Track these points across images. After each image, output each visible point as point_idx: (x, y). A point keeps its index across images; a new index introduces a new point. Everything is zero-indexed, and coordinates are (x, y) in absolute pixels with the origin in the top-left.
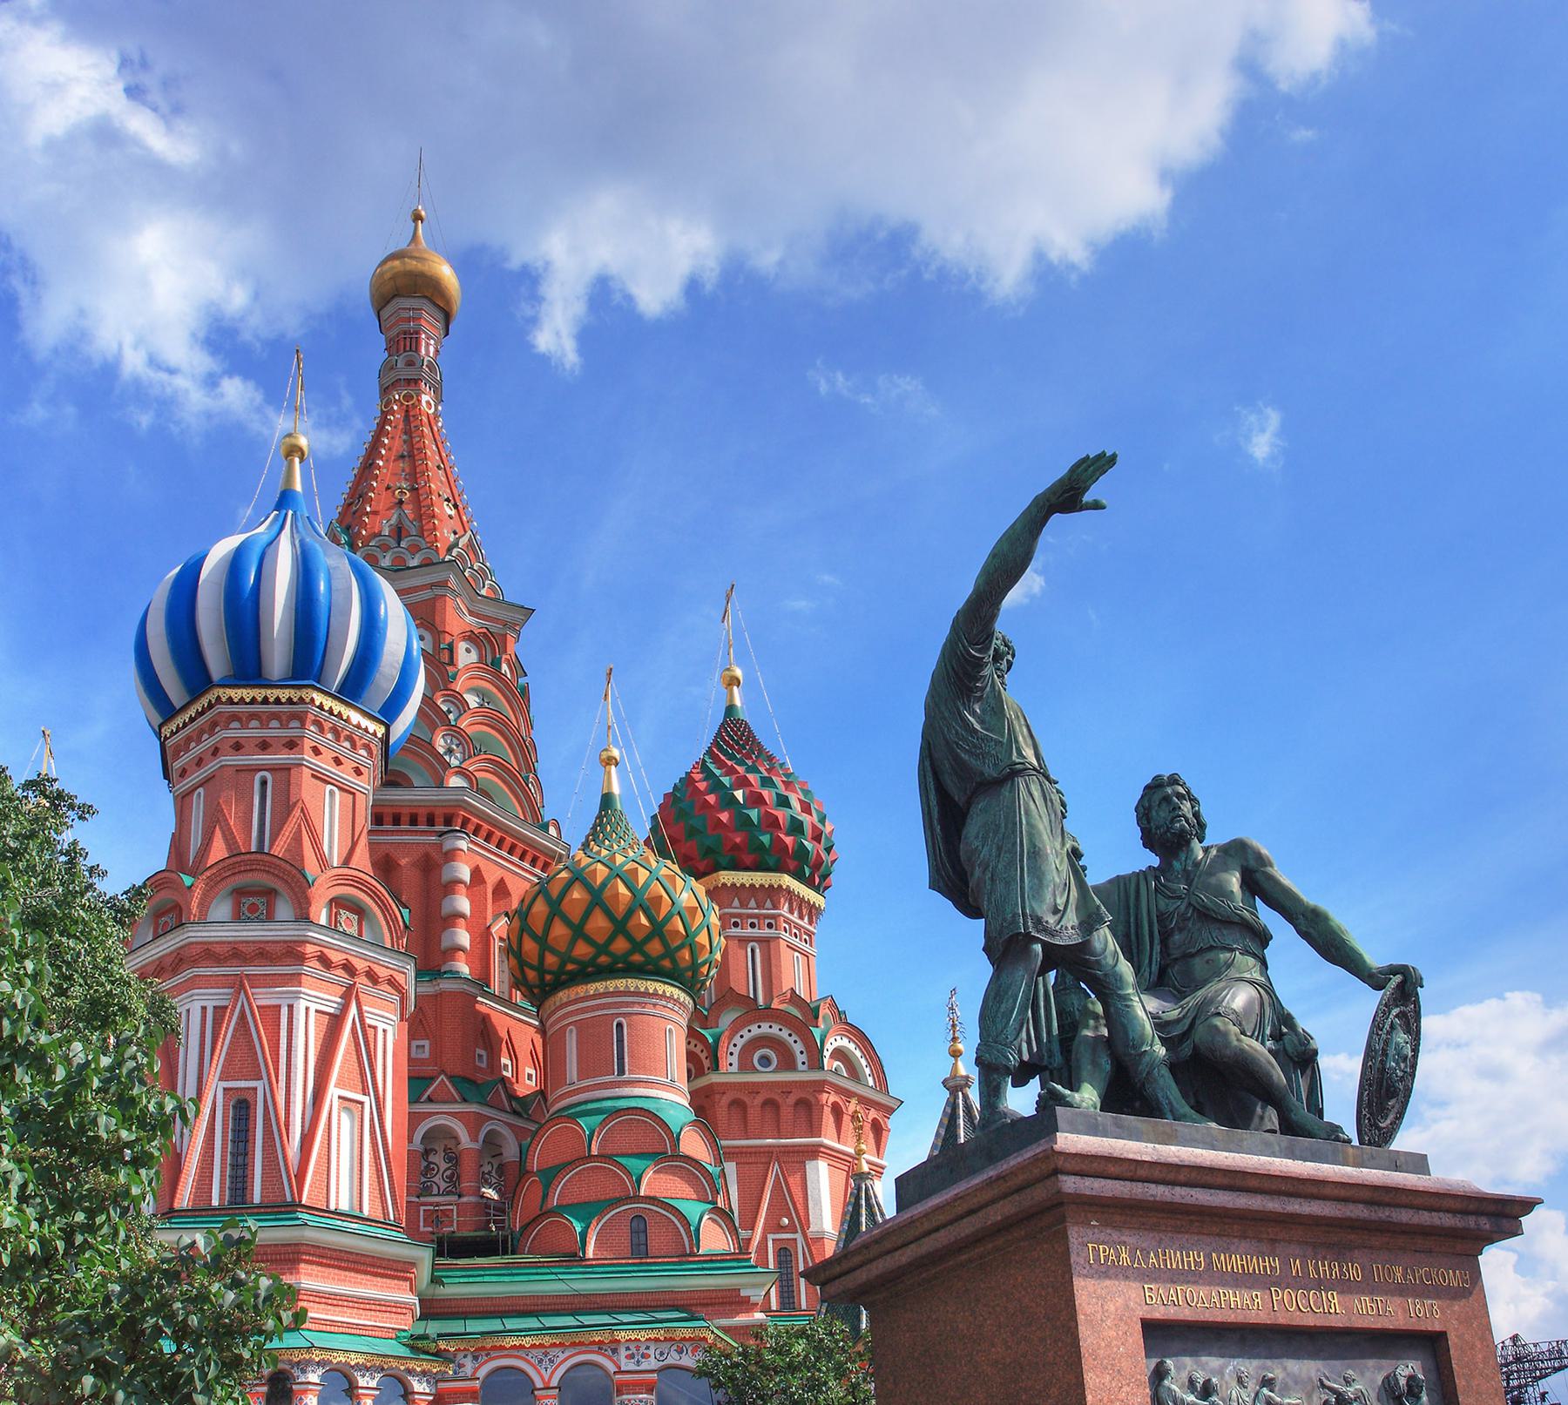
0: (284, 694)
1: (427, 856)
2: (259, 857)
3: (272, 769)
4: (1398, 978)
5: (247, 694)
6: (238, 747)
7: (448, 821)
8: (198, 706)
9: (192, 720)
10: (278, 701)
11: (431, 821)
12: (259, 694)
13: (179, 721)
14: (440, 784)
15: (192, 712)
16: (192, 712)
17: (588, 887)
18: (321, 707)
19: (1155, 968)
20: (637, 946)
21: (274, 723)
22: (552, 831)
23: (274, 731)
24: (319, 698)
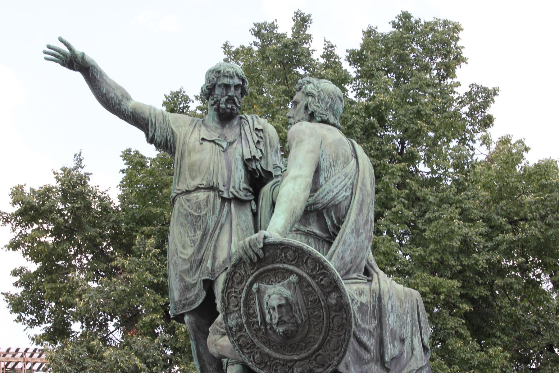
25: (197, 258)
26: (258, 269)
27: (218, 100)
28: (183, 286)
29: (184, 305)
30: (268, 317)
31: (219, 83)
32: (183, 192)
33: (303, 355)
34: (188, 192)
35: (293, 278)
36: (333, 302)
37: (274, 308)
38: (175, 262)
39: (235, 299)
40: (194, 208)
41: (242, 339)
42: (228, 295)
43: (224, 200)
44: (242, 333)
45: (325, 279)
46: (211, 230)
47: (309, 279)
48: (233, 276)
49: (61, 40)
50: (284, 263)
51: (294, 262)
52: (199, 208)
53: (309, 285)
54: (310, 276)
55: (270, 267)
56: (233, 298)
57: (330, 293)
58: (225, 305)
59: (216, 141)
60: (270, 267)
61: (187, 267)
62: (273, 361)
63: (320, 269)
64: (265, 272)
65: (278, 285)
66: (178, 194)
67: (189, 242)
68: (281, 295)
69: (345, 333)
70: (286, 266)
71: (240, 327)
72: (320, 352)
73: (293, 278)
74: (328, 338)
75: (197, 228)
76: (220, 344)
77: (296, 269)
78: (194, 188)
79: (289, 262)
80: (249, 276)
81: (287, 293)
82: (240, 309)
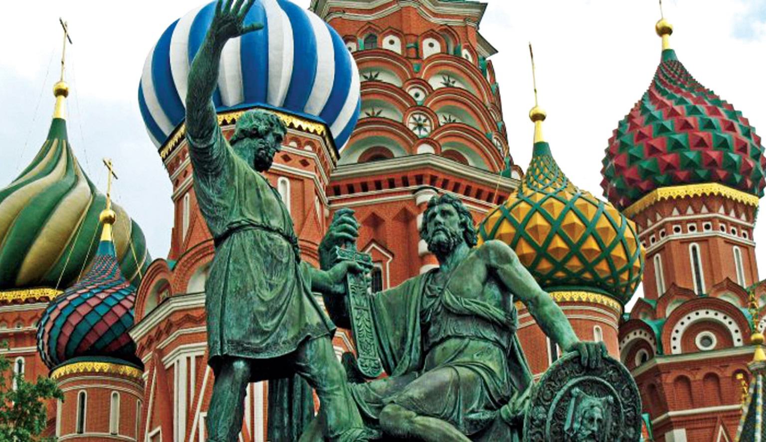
1: (405, 210)
4: (573, 353)
7: (419, 180)
9: (177, 144)
11: (406, 183)
14: (412, 154)
15: (176, 139)
16: (176, 139)
17: (512, 222)
19: (416, 355)
20: (559, 266)
22: (515, 175)
25: (275, 306)
26: (585, 375)
29: (245, 350)
31: (275, 131)
34: (269, 229)
35: (611, 398)
37: (592, 420)
38: (251, 298)
39: (550, 395)
41: (537, 435)
44: (540, 430)
46: (289, 284)
50: (608, 381)
57: (629, 426)
61: (263, 309)
64: (589, 380)
65: (596, 399)
71: (543, 422)
73: (611, 398)
76: (422, 422)
77: (614, 391)
78: (275, 229)
79: (611, 382)
80: (571, 378)
82: (550, 406)
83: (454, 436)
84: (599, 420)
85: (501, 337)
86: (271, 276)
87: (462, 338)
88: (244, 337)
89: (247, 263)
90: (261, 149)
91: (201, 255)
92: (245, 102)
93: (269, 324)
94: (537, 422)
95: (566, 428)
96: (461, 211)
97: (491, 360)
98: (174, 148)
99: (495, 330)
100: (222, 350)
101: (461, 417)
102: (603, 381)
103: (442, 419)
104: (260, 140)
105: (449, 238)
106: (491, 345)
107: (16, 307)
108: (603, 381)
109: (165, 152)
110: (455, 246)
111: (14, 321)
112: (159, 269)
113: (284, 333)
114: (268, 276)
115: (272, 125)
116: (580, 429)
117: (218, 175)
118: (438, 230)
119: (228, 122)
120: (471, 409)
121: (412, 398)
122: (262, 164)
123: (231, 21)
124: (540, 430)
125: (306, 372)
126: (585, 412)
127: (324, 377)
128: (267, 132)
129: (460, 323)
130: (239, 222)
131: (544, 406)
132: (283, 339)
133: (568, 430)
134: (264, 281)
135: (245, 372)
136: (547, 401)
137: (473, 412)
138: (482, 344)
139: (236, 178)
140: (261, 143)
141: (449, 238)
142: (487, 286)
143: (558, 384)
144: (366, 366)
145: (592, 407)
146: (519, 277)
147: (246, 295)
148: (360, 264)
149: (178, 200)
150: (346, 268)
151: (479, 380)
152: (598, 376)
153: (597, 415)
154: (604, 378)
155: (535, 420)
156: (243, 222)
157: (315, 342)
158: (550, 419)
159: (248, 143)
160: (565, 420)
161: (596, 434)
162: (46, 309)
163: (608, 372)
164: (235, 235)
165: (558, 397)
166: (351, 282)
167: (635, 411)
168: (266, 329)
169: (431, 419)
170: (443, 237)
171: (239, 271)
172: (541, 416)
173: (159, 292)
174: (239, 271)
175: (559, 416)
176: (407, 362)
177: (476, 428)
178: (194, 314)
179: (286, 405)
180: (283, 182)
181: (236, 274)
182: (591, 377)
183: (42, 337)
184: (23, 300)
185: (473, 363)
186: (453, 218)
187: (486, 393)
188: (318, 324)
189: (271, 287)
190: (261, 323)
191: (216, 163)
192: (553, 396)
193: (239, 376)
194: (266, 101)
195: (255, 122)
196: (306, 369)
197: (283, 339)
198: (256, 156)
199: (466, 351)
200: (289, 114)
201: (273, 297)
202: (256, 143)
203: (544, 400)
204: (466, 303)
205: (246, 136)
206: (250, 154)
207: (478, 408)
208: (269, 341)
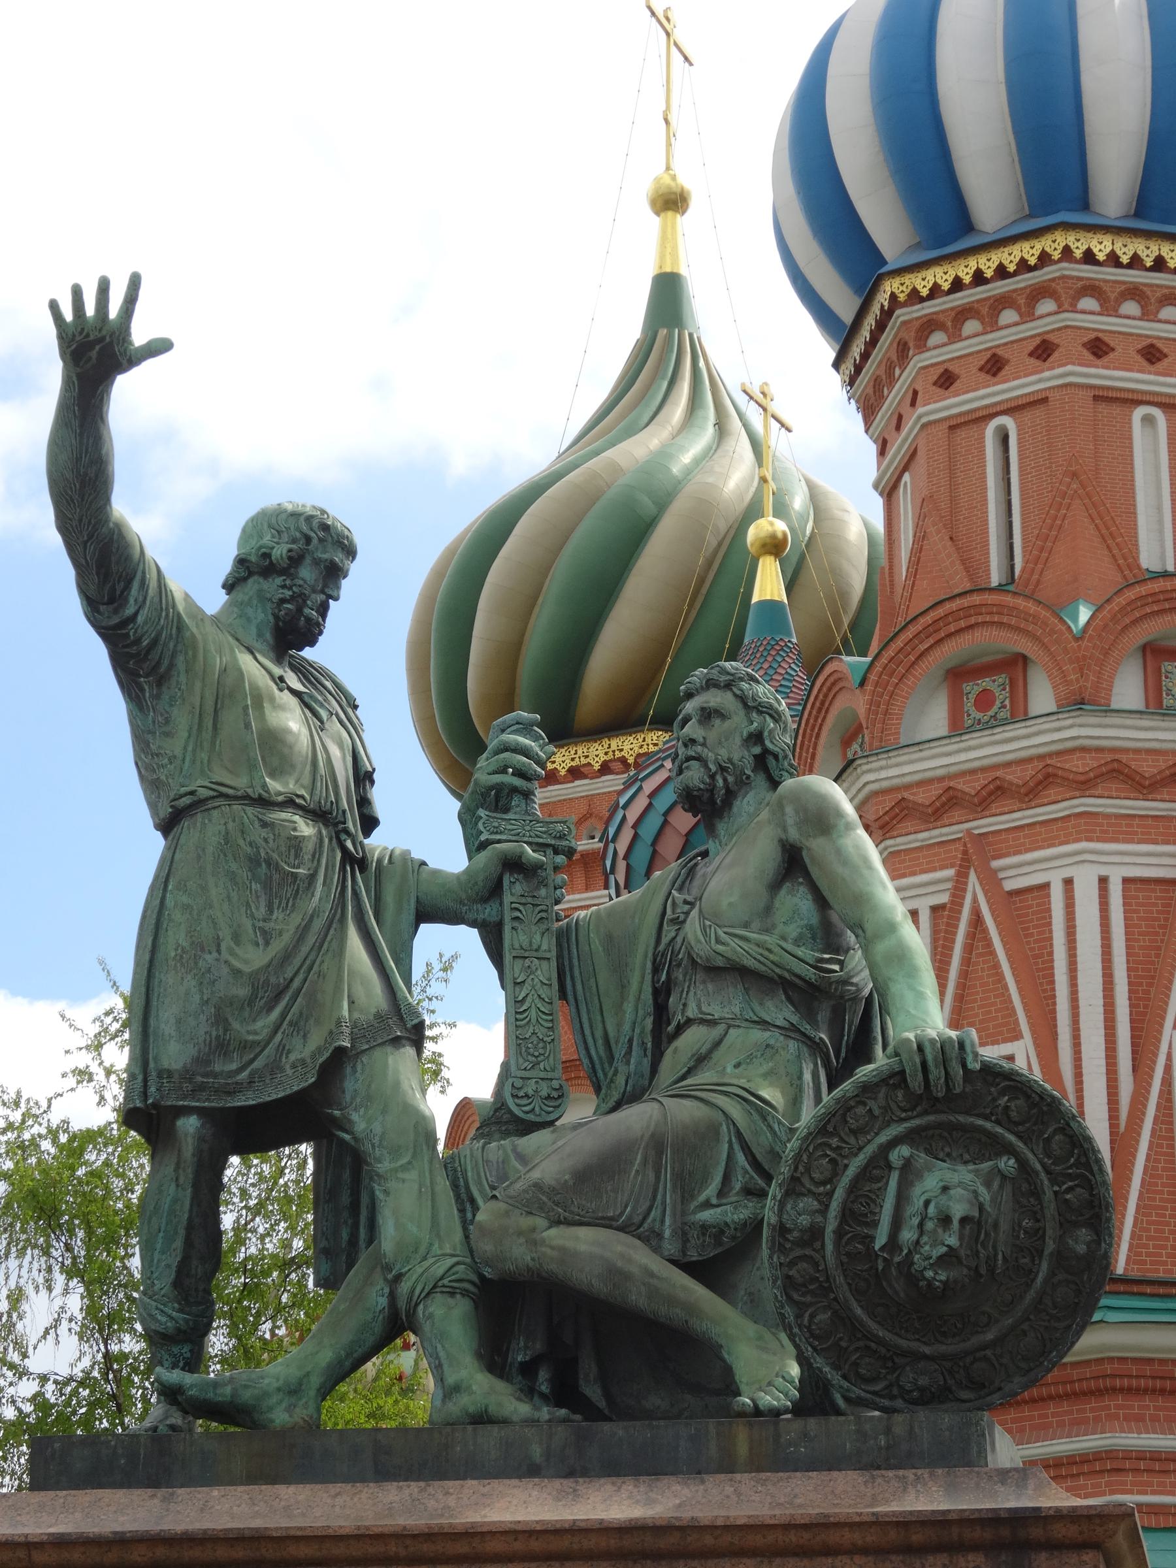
0: (1009, 257)
2: (1008, 599)
3: (1014, 409)
5: (942, 276)
6: (946, 380)
8: (870, 322)
10: (1002, 272)
12: (965, 270)
13: (856, 350)
15: (865, 333)
16: (865, 333)
18: (1089, 257)
19: (639, 1061)
21: (1008, 316)
23: (1012, 330)
24: (1079, 243)
25: (273, 980)
26: (926, 1113)
27: (301, 595)
28: (218, 1037)
30: (907, 1235)
32: (246, 797)
33: (942, 1348)
35: (1007, 1164)
36: (1081, 1249)
38: (209, 971)
39: (829, 1167)
40: (283, 849)
42: (815, 1148)
43: (347, 855)
44: (808, 1252)
45: (1078, 1189)
46: (318, 924)
47: (1043, 1175)
48: (849, 1109)
49: (135, 283)
50: (998, 1122)
51: (1021, 1128)
52: (297, 856)
53: (1036, 1193)
54: (1048, 1172)
55: (962, 1119)
56: (825, 1161)
58: (796, 1168)
59: (306, 699)
60: (962, 1119)
61: (243, 992)
62: (859, 1339)
63: (1077, 1164)
64: (939, 1125)
65: (961, 1168)
66: (222, 795)
67: (251, 931)
68: (975, 1192)
69: (1070, 1326)
70: (999, 1130)
71: (815, 1234)
72: (988, 1352)
74: (1025, 1326)
75: (277, 901)
76: (555, 1243)
78: (280, 798)
80: (887, 1124)
81: (985, 1195)
82: (830, 1195)
83: (635, 1270)
84: (964, 1220)
85: (810, 1016)
86: (270, 909)
87: (712, 1023)
88: (197, 1060)
89: (204, 888)
90: (283, 601)
91: (931, 641)
92: (1031, 216)
93: (259, 1024)
94: (796, 1234)
95: (881, 1240)
96: (751, 706)
97: (765, 1076)
98: (865, 356)
99: (789, 999)
100: (145, 1094)
101: (667, 1222)
102: (980, 1122)
103: (621, 1229)
104: (279, 580)
105: (712, 777)
106: (772, 1037)
107: (581, 787)
108: (980, 1122)
109: (848, 366)
110: (730, 795)
111: (579, 823)
112: (833, 684)
113: (297, 1041)
114: (263, 910)
115: (308, 540)
116: (917, 1242)
117: (161, 680)
118: (688, 759)
119: (989, 274)
120: (702, 1198)
121: (538, 1186)
122: (293, 631)
123: (103, 339)
124: (808, 1252)
125: (347, 1132)
126: (927, 1203)
127: (376, 1141)
128: (296, 560)
129: (710, 987)
130: (192, 793)
131: (816, 1196)
132: (293, 1057)
133: (882, 1248)
134: (247, 924)
135: (201, 1139)
136: (824, 1183)
137: (707, 1205)
138: (758, 1035)
139: (198, 685)
140: (284, 587)
141: (712, 777)
142: (783, 892)
143: (852, 1140)
144: (527, 1096)
145: (945, 1189)
146: (840, 869)
147: (196, 963)
148: (539, 847)
149: (889, 491)
150: (500, 867)
151: (724, 1127)
152: (967, 1113)
153: (958, 1211)
154: (986, 1118)
155: (789, 1231)
156: (203, 793)
157: (365, 1059)
158: (831, 1226)
159: (256, 587)
160: (875, 1224)
161: (962, 1253)
162: (620, 793)
163: (994, 1100)
164: (186, 823)
165: (851, 1172)
166: (514, 889)
167: (1092, 1189)
168: (251, 1038)
169: (583, 1232)
170: (695, 775)
171: (186, 908)
172: (804, 1220)
173: (846, 743)
174: (186, 908)
175: (857, 1216)
176: (620, 1080)
177: (719, 1243)
178: (922, 797)
179: (345, 1199)
180: (1148, 420)
181: (178, 916)
182: (943, 1117)
183: (613, 871)
184: (597, 767)
185: (719, 1088)
186: (727, 723)
187: (741, 1158)
188: (378, 1016)
189: (264, 933)
190: (236, 1025)
191: (154, 655)
192: (837, 1169)
193: (188, 1149)
194: (1085, 205)
195: (267, 539)
196: (343, 1124)
197: (293, 1057)
198: (276, 617)
199: (716, 1055)
200: (1148, 235)
201: (266, 960)
202: (273, 586)
203: (812, 1179)
204: (718, 941)
205: (251, 574)
206: (261, 616)
207: (721, 1194)
208: (257, 1064)
